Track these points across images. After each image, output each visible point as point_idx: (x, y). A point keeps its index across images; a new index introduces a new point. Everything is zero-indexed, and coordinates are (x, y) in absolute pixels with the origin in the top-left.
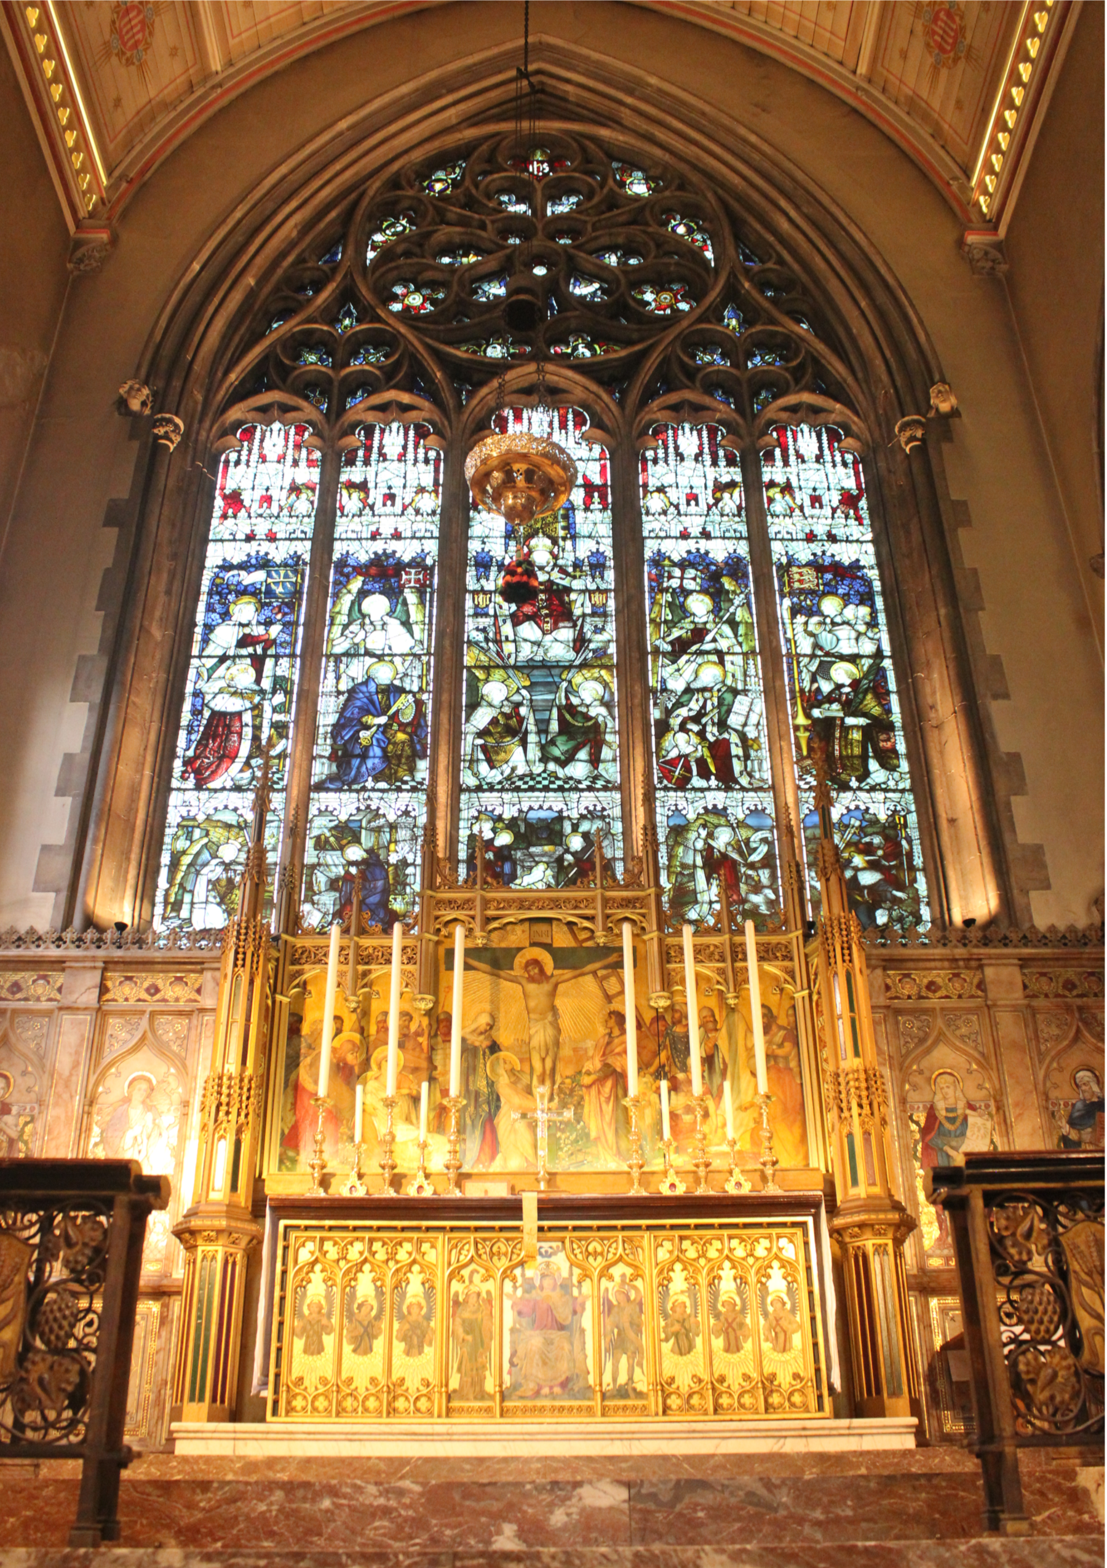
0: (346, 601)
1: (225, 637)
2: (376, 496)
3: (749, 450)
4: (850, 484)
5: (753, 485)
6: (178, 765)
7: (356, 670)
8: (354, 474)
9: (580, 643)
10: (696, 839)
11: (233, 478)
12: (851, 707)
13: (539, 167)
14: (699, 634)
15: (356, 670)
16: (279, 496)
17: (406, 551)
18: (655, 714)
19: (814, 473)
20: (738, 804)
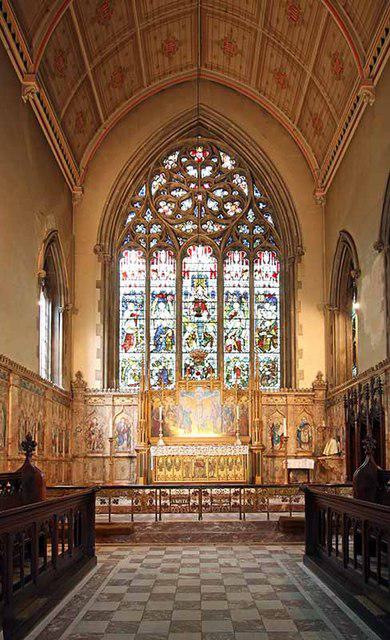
0: (155, 304)
1: (127, 314)
2: (160, 274)
3: (252, 259)
4: (276, 271)
5: (252, 271)
6: (120, 347)
7: (158, 323)
8: (153, 267)
9: (209, 316)
10: (232, 364)
11: (123, 268)
12: (268, 333)
13: (199, 154)
14: (236, 314)
15: (158, 323)
16: (136, 273)
17: (168, 290)
18: (225, 334)
19: (268, 265)
20: (242, 356)
